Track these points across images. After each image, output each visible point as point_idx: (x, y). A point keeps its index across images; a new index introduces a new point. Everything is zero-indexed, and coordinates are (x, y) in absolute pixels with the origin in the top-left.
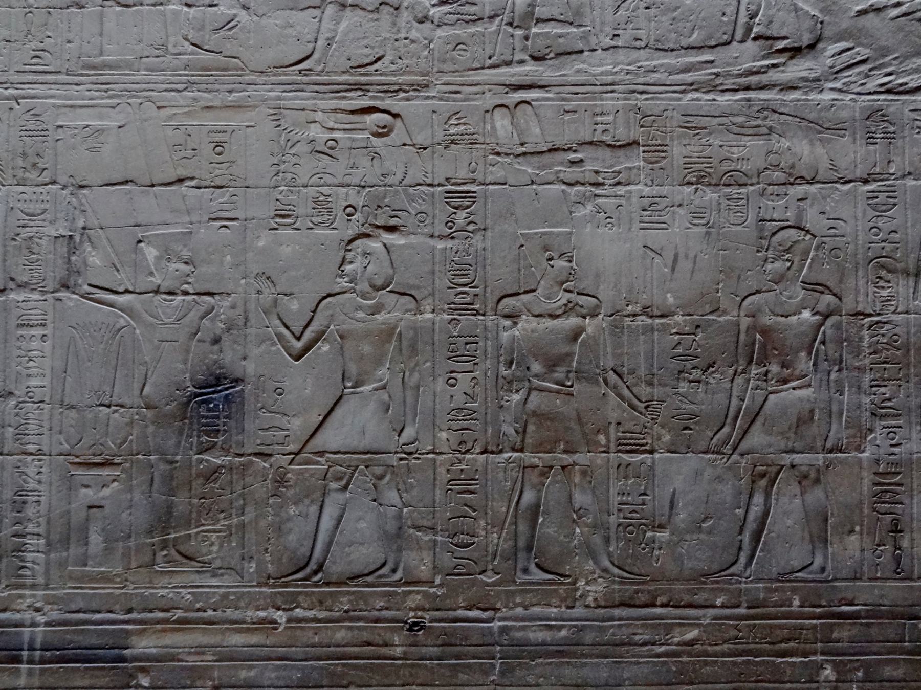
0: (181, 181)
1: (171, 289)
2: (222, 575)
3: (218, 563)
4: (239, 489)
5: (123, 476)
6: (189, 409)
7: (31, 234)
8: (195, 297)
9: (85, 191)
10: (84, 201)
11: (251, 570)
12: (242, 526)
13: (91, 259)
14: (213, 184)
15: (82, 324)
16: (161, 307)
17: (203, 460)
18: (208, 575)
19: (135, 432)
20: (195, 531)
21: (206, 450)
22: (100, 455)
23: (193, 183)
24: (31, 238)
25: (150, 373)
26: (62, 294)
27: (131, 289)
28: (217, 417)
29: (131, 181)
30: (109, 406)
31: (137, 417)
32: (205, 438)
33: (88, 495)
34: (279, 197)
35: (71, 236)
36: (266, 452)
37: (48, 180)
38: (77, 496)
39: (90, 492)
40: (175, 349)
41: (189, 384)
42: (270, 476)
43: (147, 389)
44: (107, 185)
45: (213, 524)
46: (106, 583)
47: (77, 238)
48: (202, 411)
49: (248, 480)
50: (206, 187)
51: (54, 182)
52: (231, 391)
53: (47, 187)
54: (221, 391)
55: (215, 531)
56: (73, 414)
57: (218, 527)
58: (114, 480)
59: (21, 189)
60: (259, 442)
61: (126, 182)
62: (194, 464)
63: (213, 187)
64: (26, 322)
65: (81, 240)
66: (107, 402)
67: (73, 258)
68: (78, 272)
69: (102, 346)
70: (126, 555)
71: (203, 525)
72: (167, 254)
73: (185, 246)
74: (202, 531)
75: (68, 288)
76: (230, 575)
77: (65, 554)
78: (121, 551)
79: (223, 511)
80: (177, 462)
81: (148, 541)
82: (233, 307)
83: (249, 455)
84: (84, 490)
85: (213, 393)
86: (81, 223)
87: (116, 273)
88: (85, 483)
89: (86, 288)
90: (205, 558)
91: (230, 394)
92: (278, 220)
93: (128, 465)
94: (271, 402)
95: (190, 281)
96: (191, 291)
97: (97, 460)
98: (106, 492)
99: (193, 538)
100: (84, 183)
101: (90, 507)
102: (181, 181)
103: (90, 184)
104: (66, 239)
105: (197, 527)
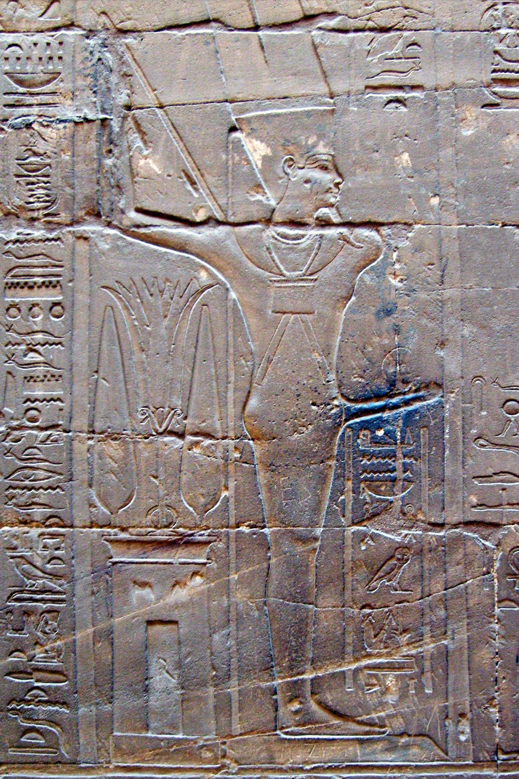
0: (308, 18)
1: (296, 216)
2: (407, 746)
3: (398, 724)
4: (437, 587)
5: (213, 565)
6: (337, 440)
7: (32, 119)
8: (344, 230)
9: (129, 40)
10: (127, 57)
11: (463, 738)
12: (445, 653)
13: (142, 162)
14: (370, 24)
15: (127, 282)
16: (277, 249)
17: (365, 535)
18: (379, 746)
19: (232, 484)
20: (353, 666)
21: (374, 515)
22: (167, 527)
23: (333, 23)
24: (29, 126)
25: (258, 373)
26: (90, 228)
27: (219, 216)
28: (393, 455)
29: (216, 20)
30: (181, 435)
31: (237, 455)
32: (367, 495)
33: (144, 600)
34: (499, 47)
35: (103, 120)
36: (489, 519)
37: (59, 21)
38: (125, 603)
39: (146, 592)
40: (307, 328)
41: (335, 392)
42: (497, 565)
43: (253, 402)
44: (170, 28)
45: (389, 654)
46: (185, 760)
47: (115, 125)
48: (363, 440)
49: (454, 571)
50: (357, 30)
51: (70, 26)
52: (417, 405)
53: (58, 33)
54: (396, 406)
55: (391, 667)
56: (113, 448)
57: (397, 659)
58: (195, 574)
59: (10, 38)
60: (474, 500)
61: (206, 22)
62: (349, 542)
63: (372, 30)
64: (22, 280)
65: (121, 127)
66: (177, 427)
67: (109, 162)
68: (118, 186)
69: (166, 322)
70: (223, 706)
71: (369, 656)
72: (288, 151)
73: (321, 137)
74: (368, 667)
75: (98, 215)
76: (420, 746)
77: (108, 707)
78: (211, 702)
79: (405, 631)
80: (316, 539)
81: (264, 685)
82: (418, 249)
83: (456, 526)
84: (137, 592)
85: (382, 409)
86: (122, 99)
87: (189, 187)
88: (141, 578)
89: (133, 215)
90: (374, 715)
91: (416, 411)
92: (498, 89)
93: (221, 545)
94: (494, 426)
95: (332, 200)
96: (336, 219)
97: (162, 534)
98: (181, 594)
99: (349, 680)
100: (128, 25)
101: (150, 623)
102: (308, 18)
103: (140, 28)
104: (95, 127)
105: (357, 660)
